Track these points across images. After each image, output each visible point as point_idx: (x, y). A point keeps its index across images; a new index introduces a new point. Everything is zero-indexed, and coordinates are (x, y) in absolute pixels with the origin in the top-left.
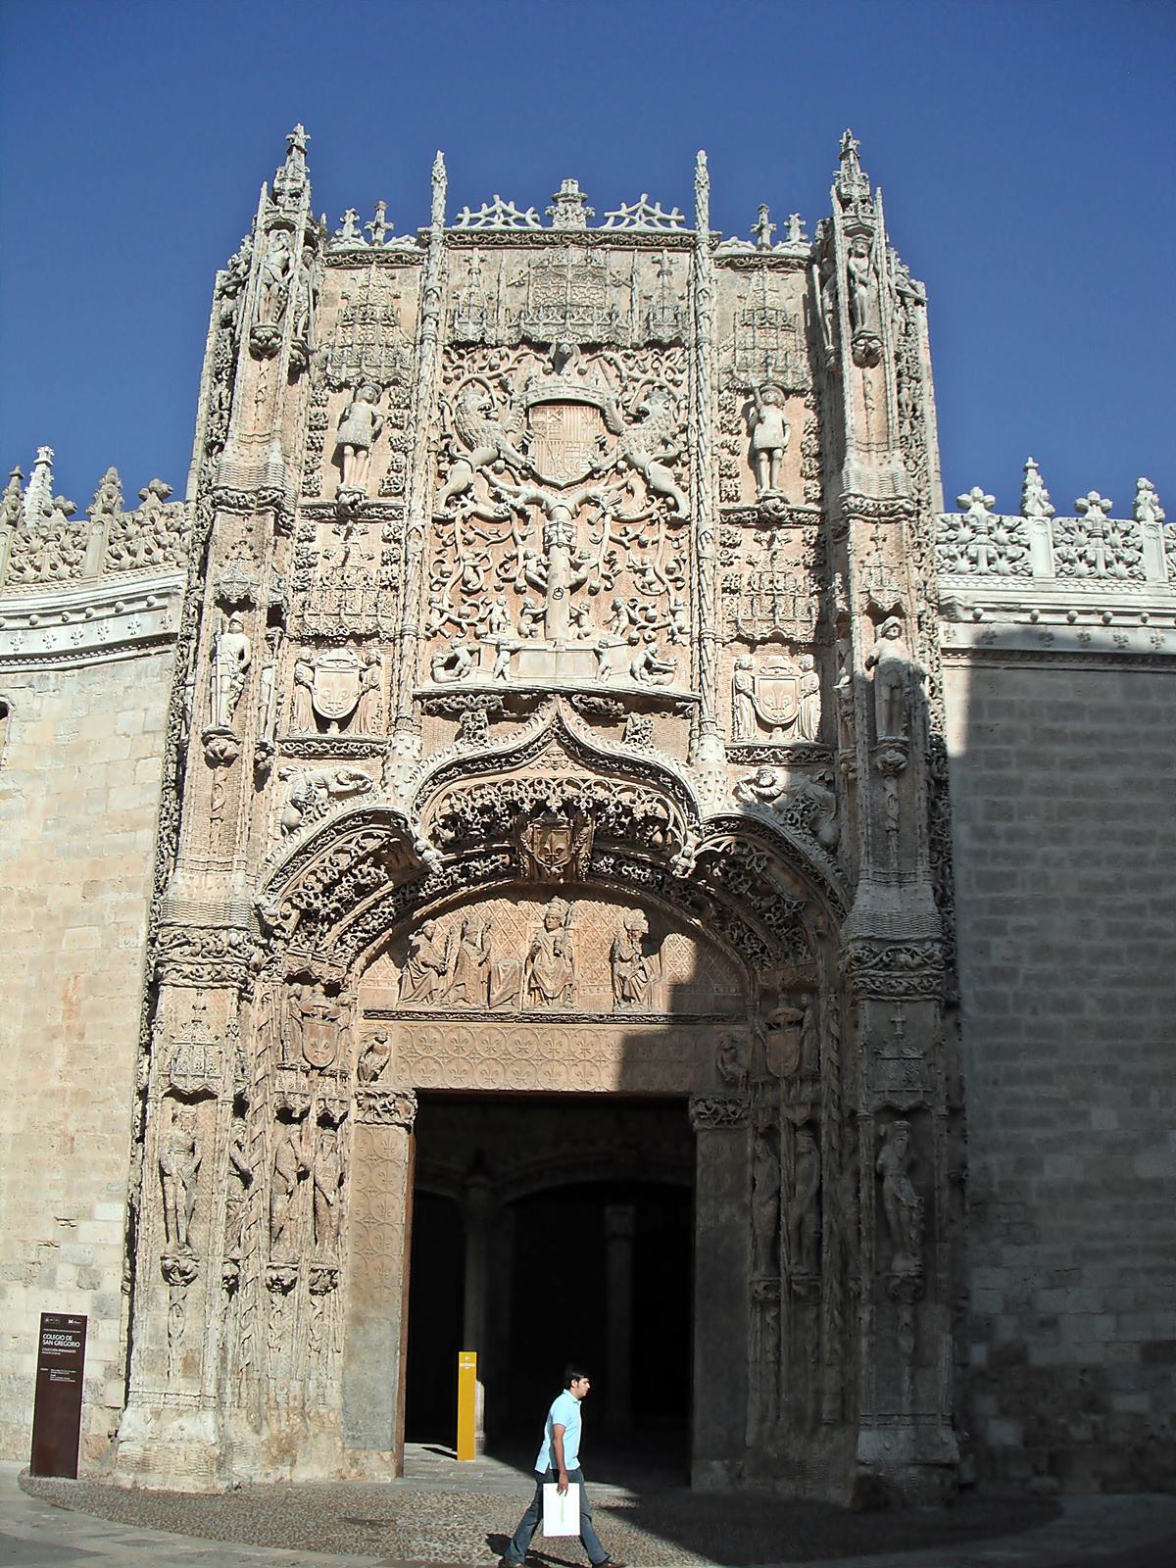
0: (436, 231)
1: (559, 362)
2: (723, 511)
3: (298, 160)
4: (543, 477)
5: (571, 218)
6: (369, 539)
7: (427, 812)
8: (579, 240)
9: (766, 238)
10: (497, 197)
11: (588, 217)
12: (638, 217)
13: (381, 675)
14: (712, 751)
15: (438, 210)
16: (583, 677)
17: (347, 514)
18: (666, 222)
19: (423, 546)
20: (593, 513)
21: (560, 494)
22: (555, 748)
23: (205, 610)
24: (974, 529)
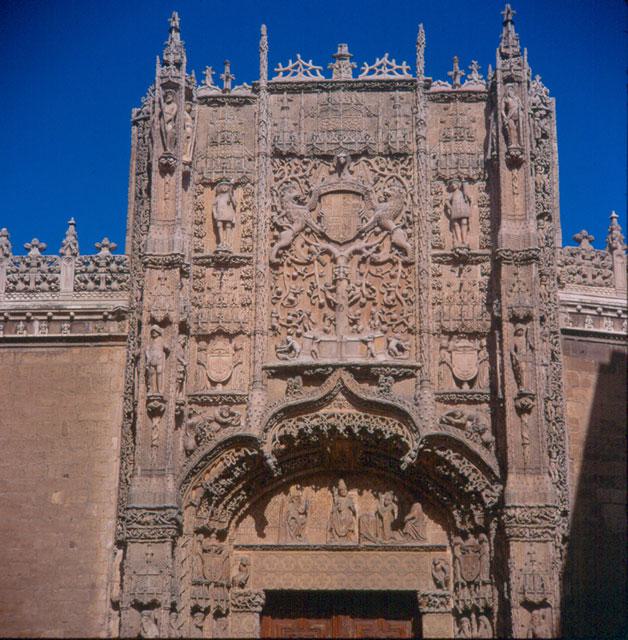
0: (263, 82)
1: (340, 168)
2: (435, 256)
3: (176, 36)
4: (333, 237)
5: (343, 71)
6: (232, 278)
7: (270, 436)
8: (351, 87)
9: (458, 81)
10: (299, 56)
11: (353, 69)
12: (385, 68)
13: (244, 356)
14: (428, 396)
15: (264, 70)
16: (356, 358)
17: (222, 263)
18: (400, 71)
19: (265, 282)
20: (358, 258)
21: (342, 248)
22: (341, 396)
23: (143, 326)
24: (583, 257)
